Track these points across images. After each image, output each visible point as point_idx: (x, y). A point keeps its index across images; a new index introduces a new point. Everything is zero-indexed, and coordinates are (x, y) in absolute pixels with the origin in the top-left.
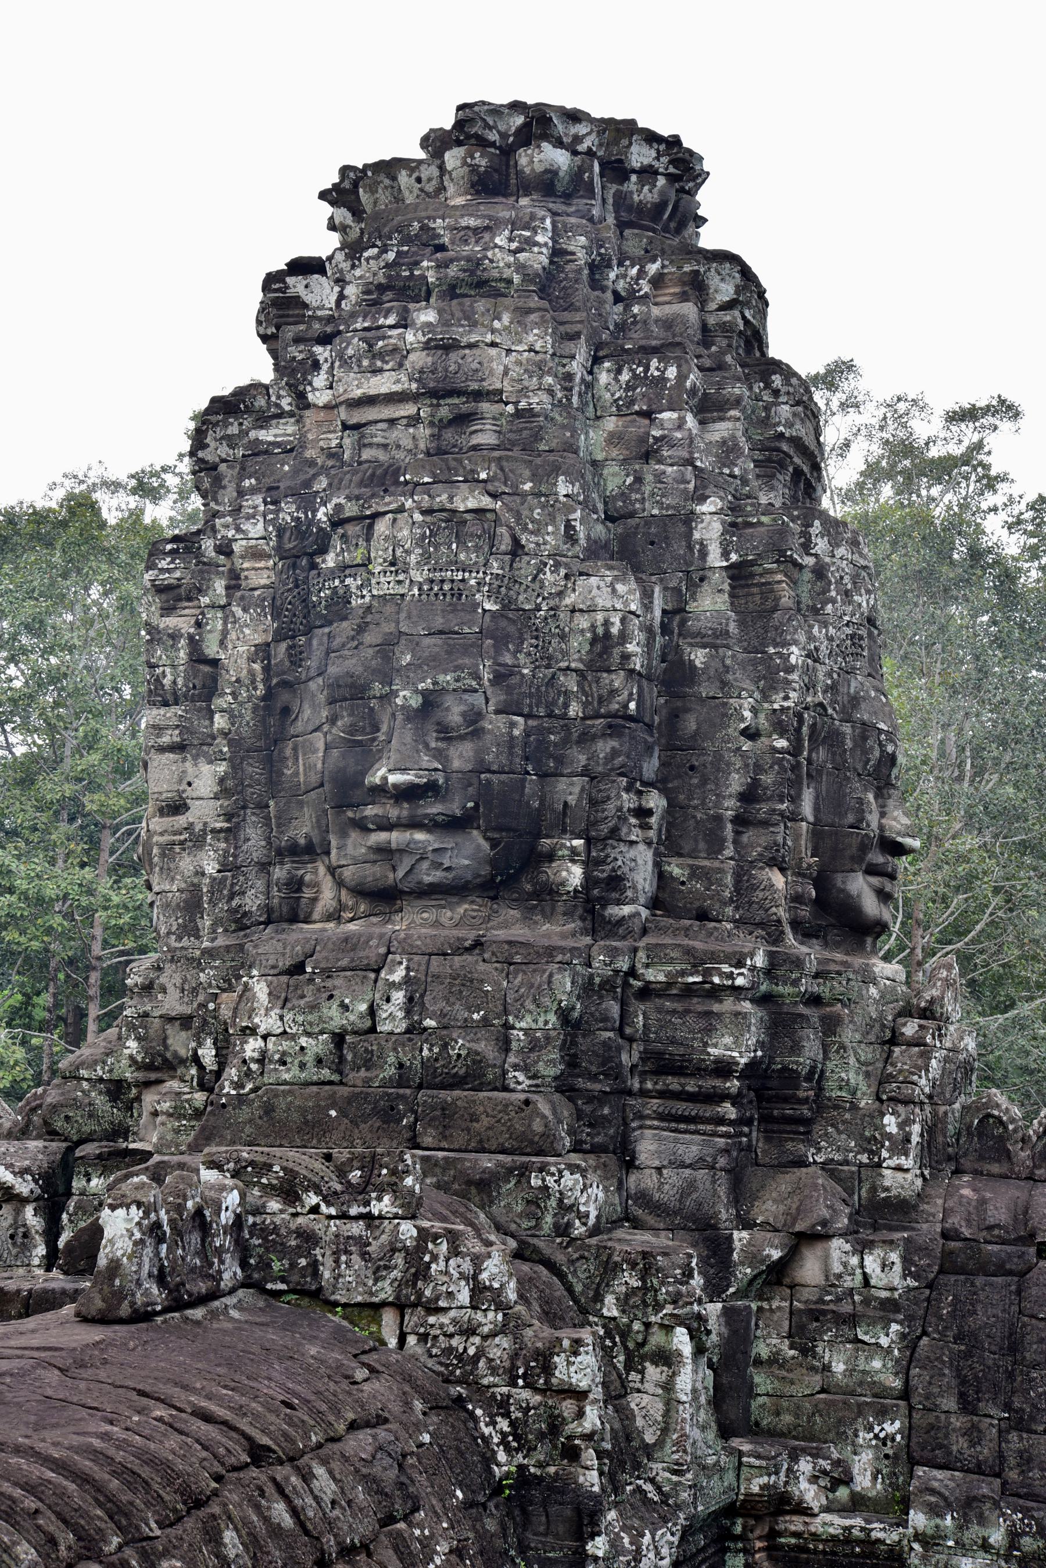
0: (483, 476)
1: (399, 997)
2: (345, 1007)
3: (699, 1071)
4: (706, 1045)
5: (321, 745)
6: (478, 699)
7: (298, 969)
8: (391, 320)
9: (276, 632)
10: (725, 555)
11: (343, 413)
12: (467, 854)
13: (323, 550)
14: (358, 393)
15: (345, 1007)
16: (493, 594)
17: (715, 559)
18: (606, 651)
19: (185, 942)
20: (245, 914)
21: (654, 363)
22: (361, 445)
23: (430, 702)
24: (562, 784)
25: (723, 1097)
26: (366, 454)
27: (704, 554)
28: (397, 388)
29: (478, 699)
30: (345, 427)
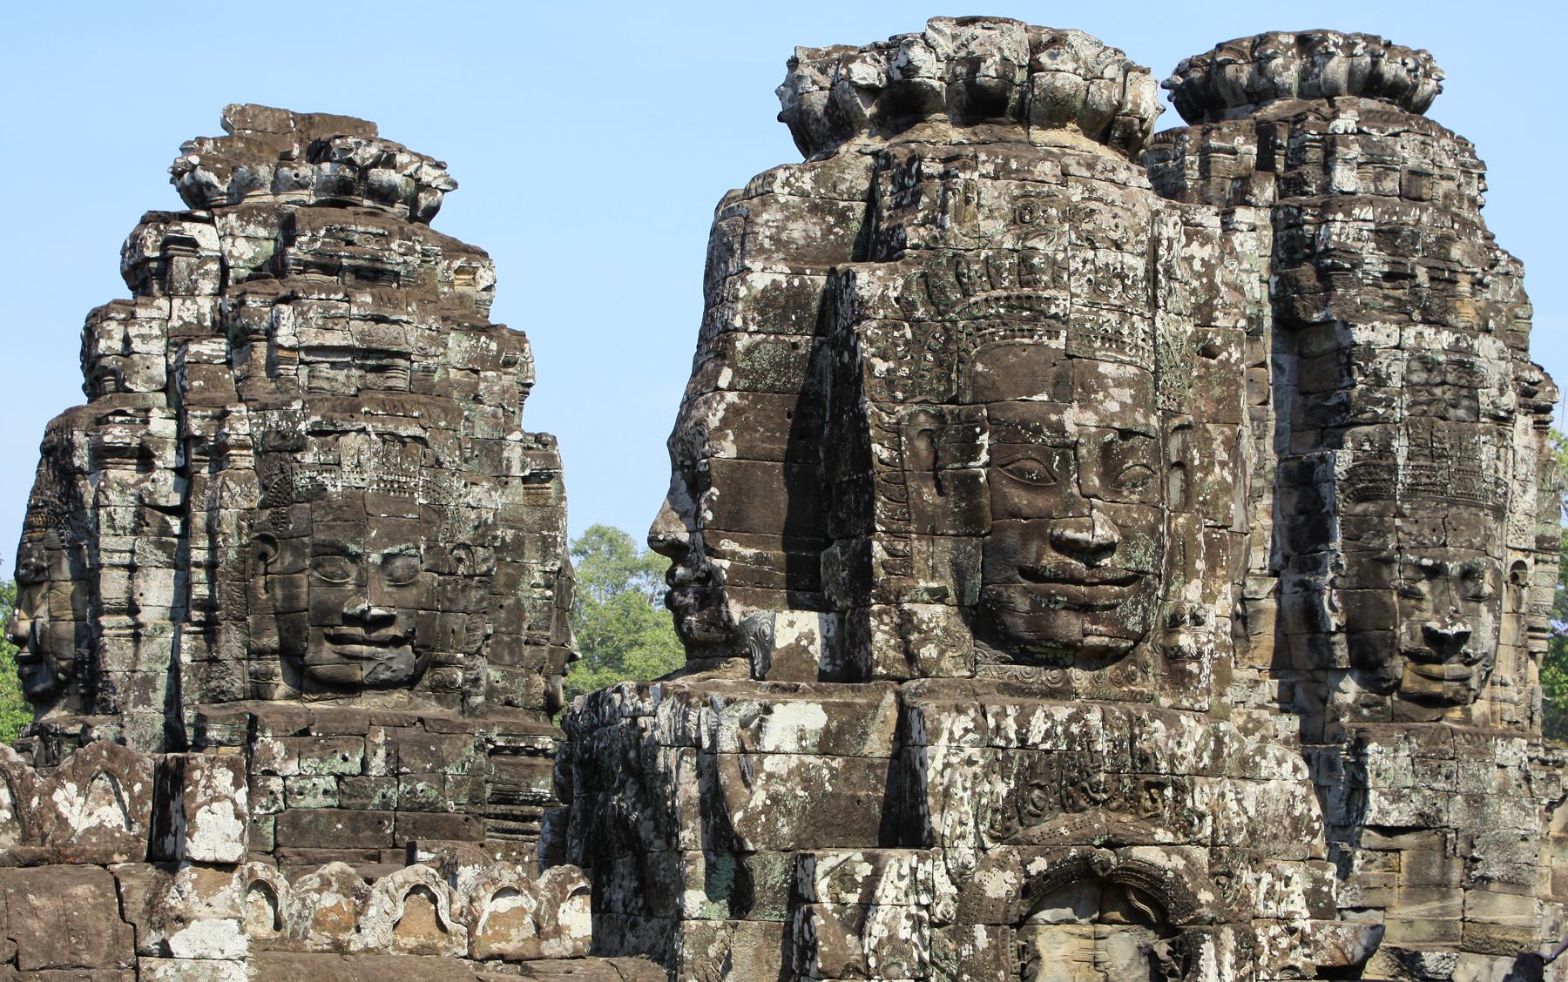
0: (416, 414)
1: (382, 752)
2: (345, 759)
3: (525, 803)
4: (529, 786)
5: (305, 582)
6: (416, 561)
7: (305, 733)
8: (340, 296)
9: (263, 502)
10: (523, 469)
11: (302, 355)
12: (402, 660)
13: (301, 448)
14: (315, 343)
15: (345, 759)
16: (427, 494)
17: (516, 470)
18: (483, 536)
19: (140, 708)
20: (223, 692)
21: (483, 339)
22: (311, 376)
23: (388, 558)
24: (451, 617)
25: (533, 818)
26: (315, 383)
27: (509, 468)
28: (343, 343)
29: (416, 561)
30: (302, 362)
